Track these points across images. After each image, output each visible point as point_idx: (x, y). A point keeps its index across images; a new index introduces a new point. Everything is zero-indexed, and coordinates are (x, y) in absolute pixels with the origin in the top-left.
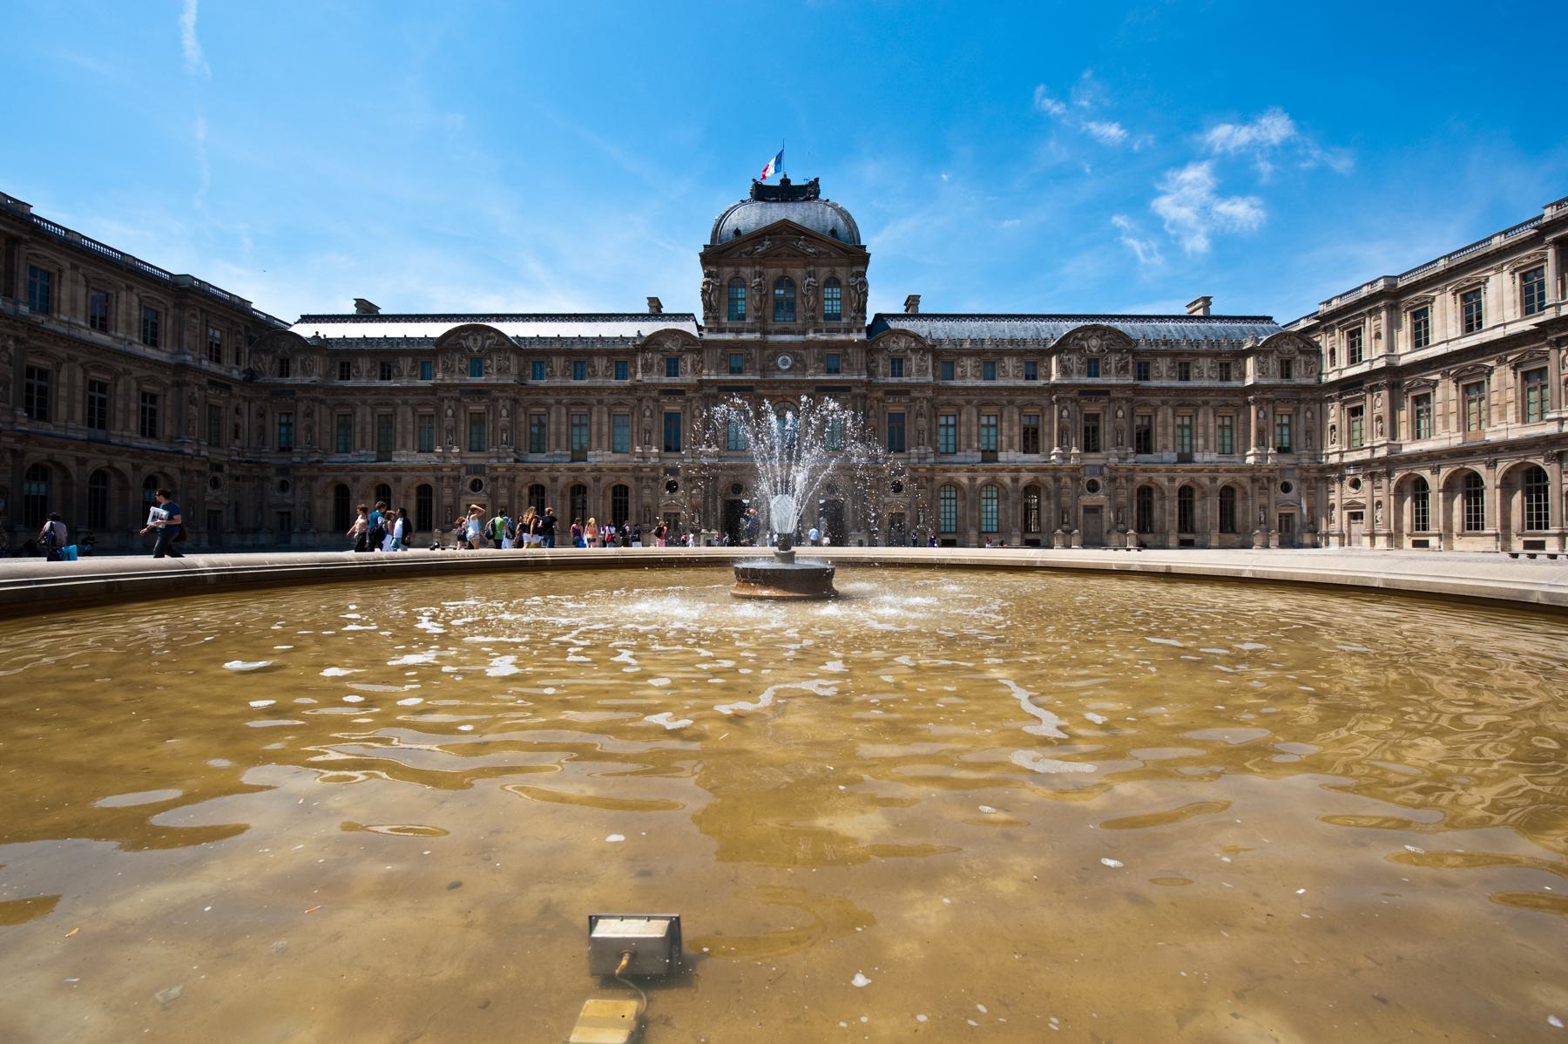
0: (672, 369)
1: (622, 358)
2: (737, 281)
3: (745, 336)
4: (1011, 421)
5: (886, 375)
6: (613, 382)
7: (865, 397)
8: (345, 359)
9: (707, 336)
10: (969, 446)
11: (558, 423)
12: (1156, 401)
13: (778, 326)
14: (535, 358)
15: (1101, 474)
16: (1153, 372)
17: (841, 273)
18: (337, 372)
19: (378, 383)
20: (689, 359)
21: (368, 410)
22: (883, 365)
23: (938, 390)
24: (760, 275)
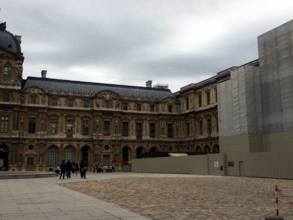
4: (78, 122)
5: (29, 103)
7: (19, 112)
10: (62, 131)
15: (110, 143)
23: (49, 109)
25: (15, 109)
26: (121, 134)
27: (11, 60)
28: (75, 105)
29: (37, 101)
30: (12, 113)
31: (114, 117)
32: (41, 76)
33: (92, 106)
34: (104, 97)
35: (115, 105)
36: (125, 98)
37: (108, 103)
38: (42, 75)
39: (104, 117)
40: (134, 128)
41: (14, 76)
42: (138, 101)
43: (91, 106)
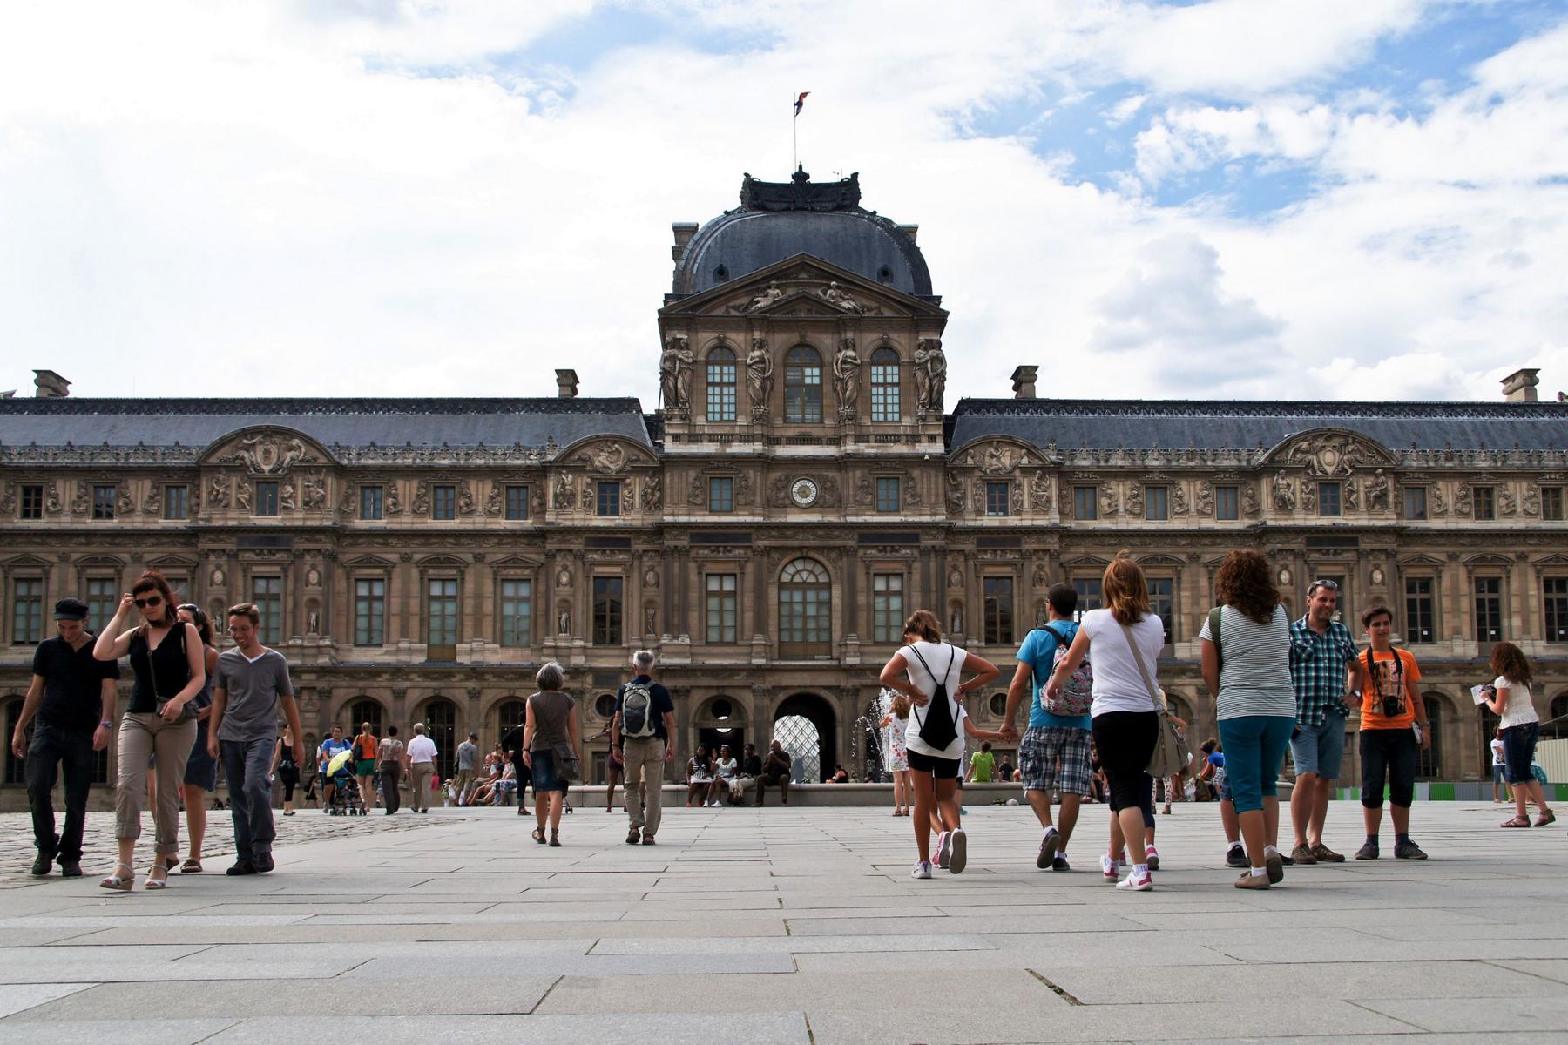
0: (608, 504)
1: (519, 480)
2: (723, 353)
3: (737, 448)
4: (1195, 587)
5: (979, 513)
6: (503, 524)
7: (942, 552)
8: (33, 481)
9: (671, 447)
11: (405, 596)
12: (1438, 554)
13: (791, 433)
14: (367, 481)
16: (1431, 504)
17: (900, 340)
18: (18, 504)
19: (91, 523)
20: (636, 488)
21: (72, 571)
22: (972, 491)
23: (1066, 535)
24: (761, 345)
25: (927, 542)
26: (1402, 636)
27: (896, 331)
28: (1178, 509)
29: (1016, 503)
30: (915, 560)
31: (1361, 555)
32: (1012, 395)
33: (1256, 512)
34: (1309, 465)
35: (1367, 499)
36: (1413, 462)
37: (1329, 492)
38: (1015, 388)
39: (1315, 556)
40: (1466, 604)
41: (913, 399)
42: (1477, 473)
43: (1247, 509)
